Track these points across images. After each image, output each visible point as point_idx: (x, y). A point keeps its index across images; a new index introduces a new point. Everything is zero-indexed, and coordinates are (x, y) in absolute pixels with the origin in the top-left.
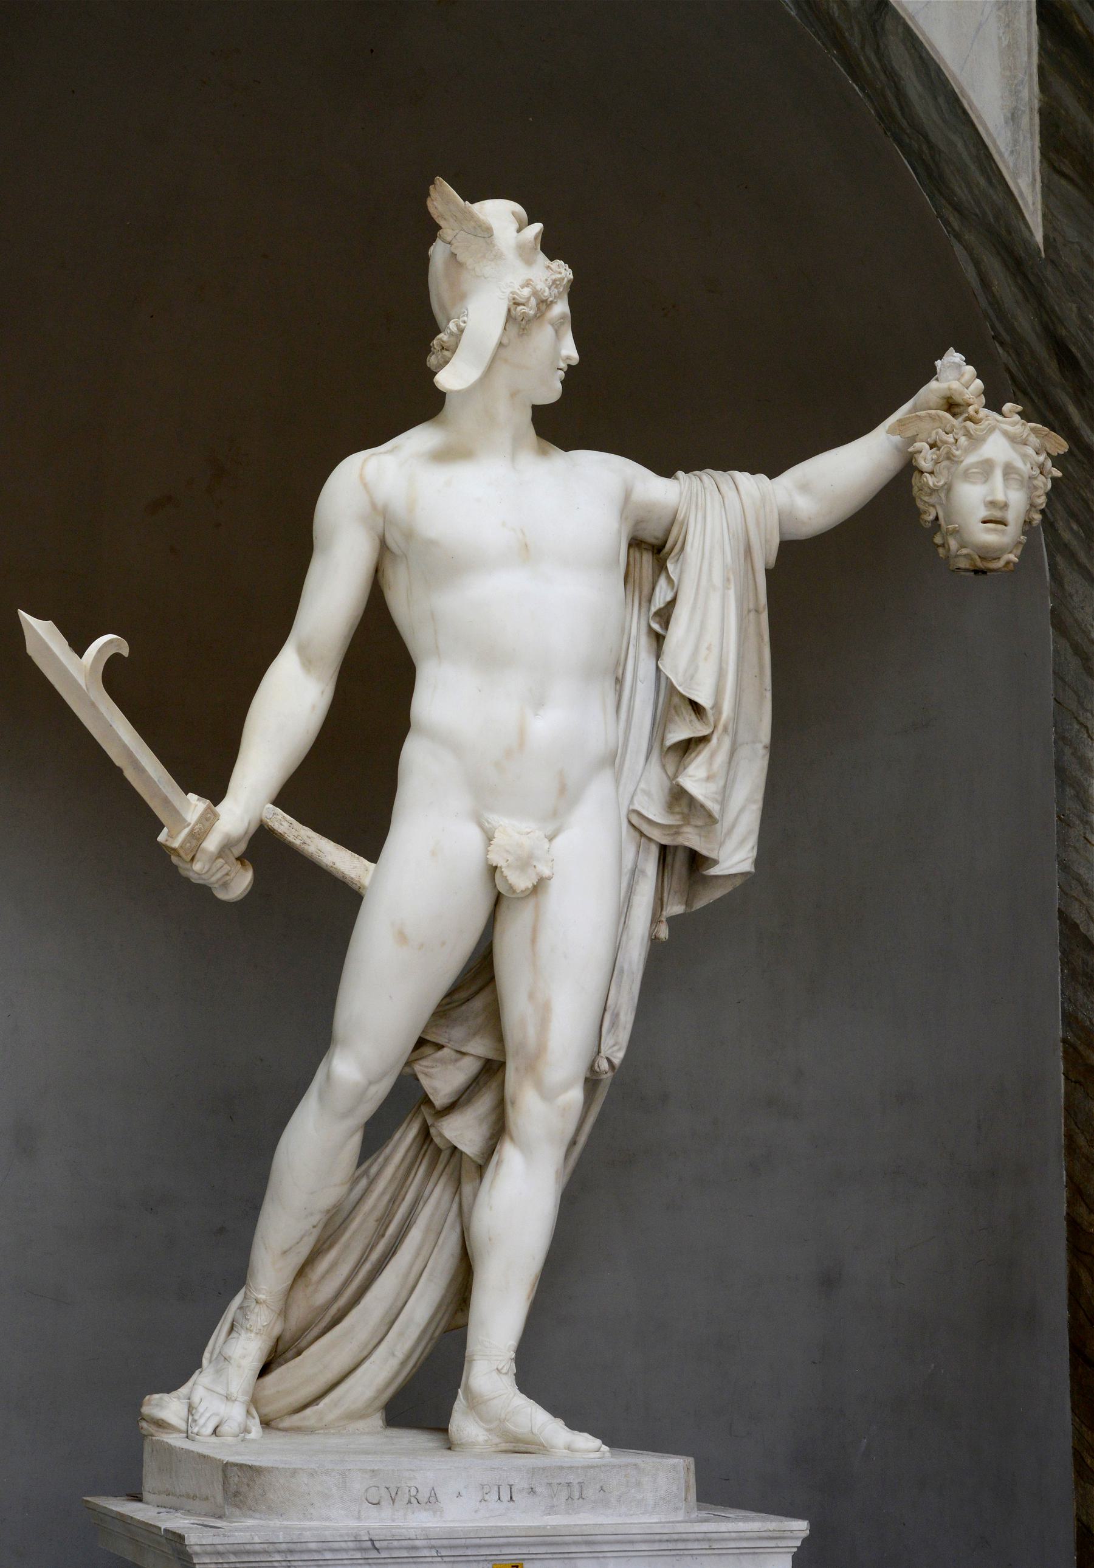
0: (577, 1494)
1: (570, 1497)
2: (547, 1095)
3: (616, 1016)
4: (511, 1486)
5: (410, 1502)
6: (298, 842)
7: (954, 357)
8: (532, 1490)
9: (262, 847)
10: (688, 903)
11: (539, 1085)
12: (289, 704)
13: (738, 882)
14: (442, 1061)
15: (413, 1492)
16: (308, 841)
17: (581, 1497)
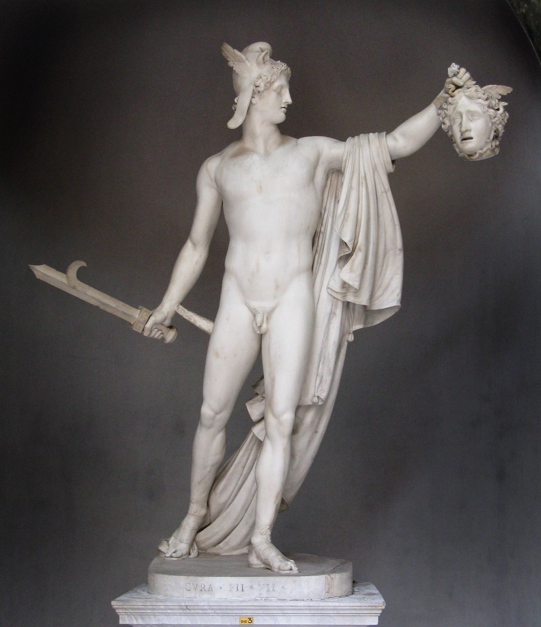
0: (271, 589)
2: (276, 417)
3: (322, 377)
4: (242, 585)
6: (187, 318)
7: (454, 68)
8: (252, 587)
10: (365, 323)
11: (273, 413)
13: (397, 310)
15: (203, 586)
16: (191, 318)
17: (273, 590)
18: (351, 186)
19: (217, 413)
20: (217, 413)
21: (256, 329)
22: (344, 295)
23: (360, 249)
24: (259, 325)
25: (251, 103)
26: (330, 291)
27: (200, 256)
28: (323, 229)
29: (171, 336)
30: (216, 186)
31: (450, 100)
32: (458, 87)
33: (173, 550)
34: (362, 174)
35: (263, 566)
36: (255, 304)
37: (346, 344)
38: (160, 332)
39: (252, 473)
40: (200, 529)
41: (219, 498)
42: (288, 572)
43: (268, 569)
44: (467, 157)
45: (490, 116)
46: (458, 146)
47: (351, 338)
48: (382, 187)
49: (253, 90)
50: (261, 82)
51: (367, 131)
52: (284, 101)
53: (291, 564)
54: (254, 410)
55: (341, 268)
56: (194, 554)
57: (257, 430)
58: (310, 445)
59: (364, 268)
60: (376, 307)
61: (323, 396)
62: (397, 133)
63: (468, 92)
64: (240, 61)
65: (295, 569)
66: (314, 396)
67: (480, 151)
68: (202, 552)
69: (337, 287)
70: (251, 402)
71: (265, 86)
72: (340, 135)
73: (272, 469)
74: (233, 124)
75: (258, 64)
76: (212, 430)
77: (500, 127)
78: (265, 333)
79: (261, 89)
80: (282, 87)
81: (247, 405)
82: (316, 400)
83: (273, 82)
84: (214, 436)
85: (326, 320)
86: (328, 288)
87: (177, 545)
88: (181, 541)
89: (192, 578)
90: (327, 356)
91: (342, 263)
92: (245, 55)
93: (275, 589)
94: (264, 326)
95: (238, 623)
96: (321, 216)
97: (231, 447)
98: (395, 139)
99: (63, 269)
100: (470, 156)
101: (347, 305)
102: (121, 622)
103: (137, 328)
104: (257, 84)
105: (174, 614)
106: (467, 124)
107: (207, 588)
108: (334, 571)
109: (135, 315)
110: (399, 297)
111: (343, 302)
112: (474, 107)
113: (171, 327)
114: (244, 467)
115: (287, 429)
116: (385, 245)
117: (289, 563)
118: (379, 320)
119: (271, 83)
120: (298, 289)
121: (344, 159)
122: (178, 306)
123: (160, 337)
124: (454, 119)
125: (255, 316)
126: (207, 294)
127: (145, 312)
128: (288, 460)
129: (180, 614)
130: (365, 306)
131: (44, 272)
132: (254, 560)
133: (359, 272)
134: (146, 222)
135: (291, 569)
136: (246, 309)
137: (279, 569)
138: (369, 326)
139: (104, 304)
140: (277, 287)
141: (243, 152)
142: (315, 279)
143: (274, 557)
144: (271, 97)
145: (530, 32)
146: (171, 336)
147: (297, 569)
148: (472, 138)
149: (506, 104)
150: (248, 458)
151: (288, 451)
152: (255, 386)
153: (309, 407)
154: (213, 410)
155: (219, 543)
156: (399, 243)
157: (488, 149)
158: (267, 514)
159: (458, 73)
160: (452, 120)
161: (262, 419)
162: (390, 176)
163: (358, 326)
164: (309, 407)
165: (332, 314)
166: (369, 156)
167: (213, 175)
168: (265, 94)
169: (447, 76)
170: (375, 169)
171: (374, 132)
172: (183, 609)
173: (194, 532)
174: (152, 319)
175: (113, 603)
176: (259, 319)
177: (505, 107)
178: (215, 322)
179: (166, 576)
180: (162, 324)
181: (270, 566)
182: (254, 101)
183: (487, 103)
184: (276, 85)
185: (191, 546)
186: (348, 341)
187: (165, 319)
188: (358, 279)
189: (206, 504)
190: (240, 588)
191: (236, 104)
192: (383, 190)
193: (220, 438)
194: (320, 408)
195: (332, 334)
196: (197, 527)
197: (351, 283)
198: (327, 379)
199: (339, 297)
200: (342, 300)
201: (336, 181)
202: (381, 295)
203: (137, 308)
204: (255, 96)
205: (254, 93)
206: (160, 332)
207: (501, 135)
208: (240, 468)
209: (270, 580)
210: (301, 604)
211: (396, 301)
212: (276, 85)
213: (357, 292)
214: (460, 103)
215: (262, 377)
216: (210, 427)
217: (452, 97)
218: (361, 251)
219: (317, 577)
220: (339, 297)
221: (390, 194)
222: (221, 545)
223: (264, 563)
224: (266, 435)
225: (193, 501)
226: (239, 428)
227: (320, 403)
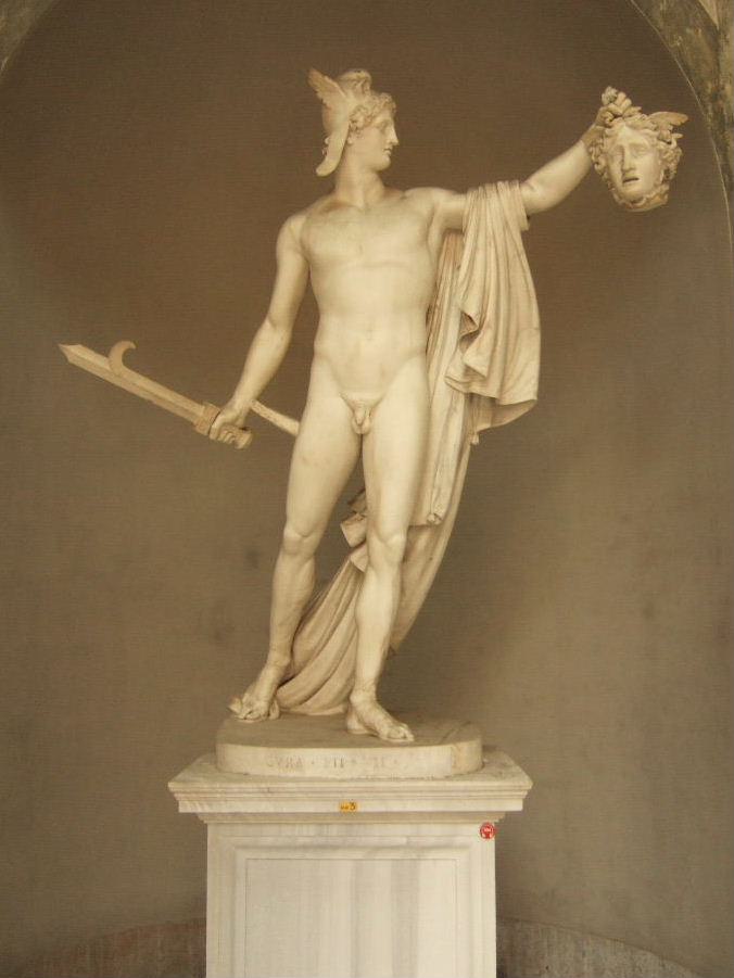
2: (383, 540)
3: (439, 490)
7: (610, 92)
8: (354, 762)
9: (252, 422)
10: (492, 422)
13: (532, 405)
19: (305, 536)
21: (356, 427)
22: (468, 384)
25: (346, 142)
28: (438, 303)
29: (244, 440)
30: (299, 249)
31: (607, 131)
32: (616, 116)
33: (249, 710)
34: (490, 230)
35: (366, 732)
36: (355, 396)
39: (349, 613)
40: (283, 682)
41: (307, 643)
43: (372, 738)
44: (630, 205)
45: (660, 151)
46: (617, 191)
47: (475, 440)
50: (359, 122)
51: (493, 180)
52: (388, 141)
53: (404, 730)
54: (352, 533)
55: (463, 352)
56: (274, 715)
57: (356, 558)
58: (423, 578)
59: (494, 351)
60: (507, 401)
61: (441, 513)
62: (534, 180)
63: (630, 121)
64: (332, 91)
65: (410, 738)
67: (648, 196)
68: (285, 712)
69: (457, 373)
70: (346, 522)
72: (460, 187)
73: (377, 605)
74: (324, 170)
75: (356, 94)
76: (298, 559)
77: (672, 166)
78: (367, 434)
79: (360, 124)
80: (386, 124)
82: (432, 518)
83: (375, 117)
84: (301, 565)
85: (444, 418)
87: (257, 700)
88: (258, 699)
91: (464, 345)
95: (336, 809)
96: (436, 287)
97: (322, 581)
98: (532, 188)
99: (104, 351)
100: (634, 202)
101: (471, 398)
102: (182, 810)
104: (354, 118)
105: (251, 799)
106: (629, 161)
107: (295, 761)
108: (458, 739)
109: (198, 412)
110: (536, 388)
111: (466, 394)
112: (640, 139)
113: (244, 429)
114: (338, 604)
115: (397, 555)
117: (402, 729)
118: (508, 419)
119: (373, 117)
120: (408, 378)
121: (466, 213)
124: (612, 157)
125: (354, 411)
127: (212, 409)
128: (398, 592)
129: (260, 800)
130: (493, 400)
131: (79, 354)
132: (354, 724)
133: (488, 354)
134: (214, 294)
135: (405, 737)
136: (342, 400)
137: (389, 737)
140: (383, 374)
141: (336, 206)
142: (430, 363)
143: (381, 720)
144: (372, 135)
145: (686, 67)
146: (244, 440)
147: (411, 736)
148: (637, 179)
149: (680, 136)
150: (342, 595)
151: (398, 584)
152: (351, 503)
153: (422, 528)
154: (300, 534)
156: (536, 321)
157: (657, 194)
158: (370, 665)
159: (616, 98)
160: (609, 158)
161: (363, 542)
162: (524, 234)
164: (422, 528)
165: (451, 410)
166: (497, 212)
168: (366, 131)
169: (601, 104)
171: (503, 180)
172: (263, 792)
173: (276, 686)
174: (220, 418)
175: (171, 785)
176: (360, 415)
177: (678, 141)
178: (303, 419)
179: (240, 747)
180: (232, 423)
181: (376, 732)
182: (350, 142)
183: (656, 133)
184: (379, 120)
185: (271, 703)
186: (471, 445)
187: (237, 419)
188: (487, 364)
189: (288, 652)
190: (338, 762)
191: (327, 146)
193: (308, 567)
194: (434, 528)
195: (452, 435)
196: (277, 681)
197: (478, 368)
198: (447, 491)
199: (460, 387)
200: (464, 391)
202: (512, 387)
203: (201, 403)
204: (352, 134)
205: (350, 130)
207: (671, 178)
208: (333, 606)
210: (421, 784)
212: (379, 120)
213: (484, 380)
214: (621, 135)
215: (363, 490)
216: (294, 554)
217: (610, 127)
219: (440, 748)
221: (524, 257)
222: (309, 703)
224: (369, 563)
226: (332, 554)
227: (438, 522)
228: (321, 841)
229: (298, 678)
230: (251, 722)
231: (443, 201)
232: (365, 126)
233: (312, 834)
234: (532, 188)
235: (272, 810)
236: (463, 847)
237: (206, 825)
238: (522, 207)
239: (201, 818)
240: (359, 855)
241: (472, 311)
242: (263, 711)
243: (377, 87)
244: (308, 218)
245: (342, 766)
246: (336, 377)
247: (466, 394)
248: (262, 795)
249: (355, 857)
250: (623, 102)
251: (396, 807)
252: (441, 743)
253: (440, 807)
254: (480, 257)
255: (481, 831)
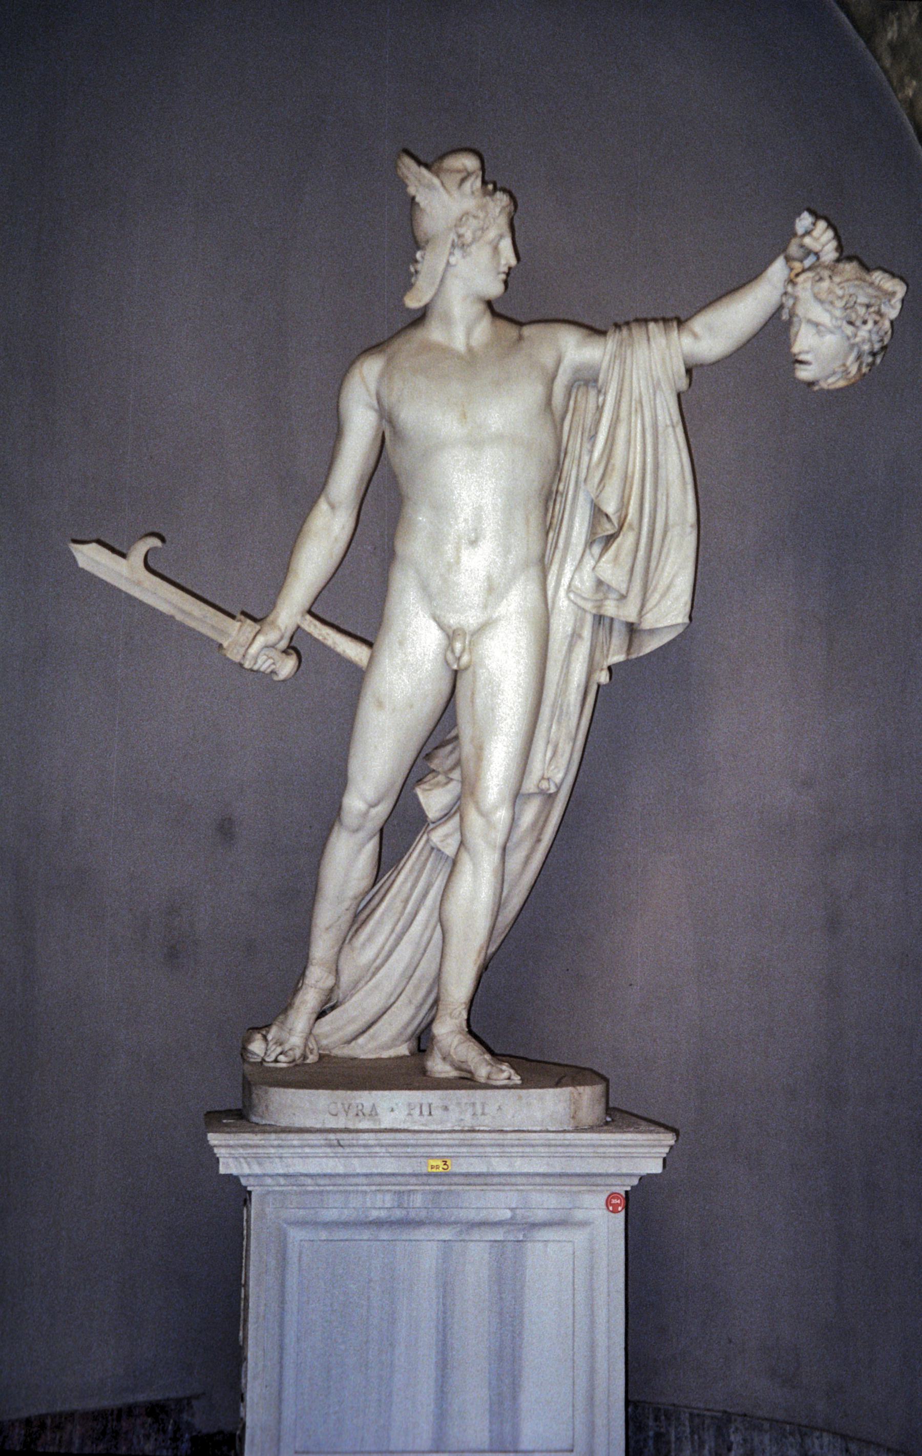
0: (479, 1111)
1: (474, 1114)
2: (483, 814)
4: (430, 1105)
5: (357, 1115)
6: (320, 638)
8: (446, 1108)
12: (326, 536)
14: (438, 785)
15: (360, 1107)
17: (483, 1114)
18: (618, 416)
19: (372, 806)
20: (372, 806)
23: (630, 525)
24: (457, 655)
25: (448, 263)
26: (572, 596)
27: (343, 528)
28: (561, 487)
29: (287, 667)
30: (376, 406)
33: (279, 1050)
37: (595, 687)
38: (271, 661)
42: (506, 1082)
43: (466, 1080)
48: (668, 417)
49: (453, 241)
54: (434, 800)
57: (442, 837)
60: (647, 624)
65: (517, 1079)
66: (543, 778)
71: (474, 233)
76: (361, 835)
78: (466, 668)
81: (419, 791)
82: (544, 785)
83: (487, 228)
84: (363, 845)
86: (569, 589)
89: (340, 1093)
90: (564, 708)
92: (438, 176)
93: (486, 1111)
94: (465, 659)
98: (695, 336)
102: (222, 1170)
103: (234, 655)
107: (367, 1111)
111: (595, 616)
114: (407, 901)
116: (667, 517)
118: (650, 645)
121: (605, 365)
122: (303, 616)
123: (269, 670)
126: (360, 597)
127: (250, 627)
133: (627, 568)
136: (434, 625)
138: (634, 656)
139: (183, 611)
144: (481, 254)
154: (366, 801)
155: (355, 1038)
163: (617, 658)
164: (530, 795)
165: (575, 636)
167: (373, 387)
168: (474, 248)
170: (656, 386)
172: (331, 1146)
173: (315, 1016)
179: (291, 1091)
180: (273, 646)
181: (470, 1072)
182: (453, 260)
184: (492, 234)
188: (626, 578)
190: (425, 1111)
192: (668, 422)
194: (550, 798)
196: (318, 1010)
197: (614, 584)
199: (588, 606)
200: (594, 611)
201: (584, 401)
205: (453, 246)
206: (271, 661)
208: (399, 905)
209: (479, 1095)
211: (682, 616)
213: (623, 597)
216: (356, 831)
218: (633, 529)
220: (588, 606)
222: (361, 1040)
223: (458, 1069)
225: (314, 961)
226: (401, 829)
227: (553, 790)
228: (398, 1214)
229: (346, 1005)
230: (284, 1065)
231: (574, 349)
232: (475, 240)
233: (388, 1205)
234: (695, 336)
235: (341, 1170)
236: (583, 1224)
237: (250, 1193)
238: (681, 358)
239: (243, 1182)
240: (446, 1234)
241: (610, 508)
242: (298, 1053)
243: (491, 184)
244: (389, 361)
245: (430, 1114)
246: (424, 588)
247: (595, 616)
248: (328, 1150)
249: (444, 1237)
250: (821, 239)
251: (501, 1166)
252: (558, 1084)
253: (557, 1166)
254: (622, 432)
255: (608, 1203)
